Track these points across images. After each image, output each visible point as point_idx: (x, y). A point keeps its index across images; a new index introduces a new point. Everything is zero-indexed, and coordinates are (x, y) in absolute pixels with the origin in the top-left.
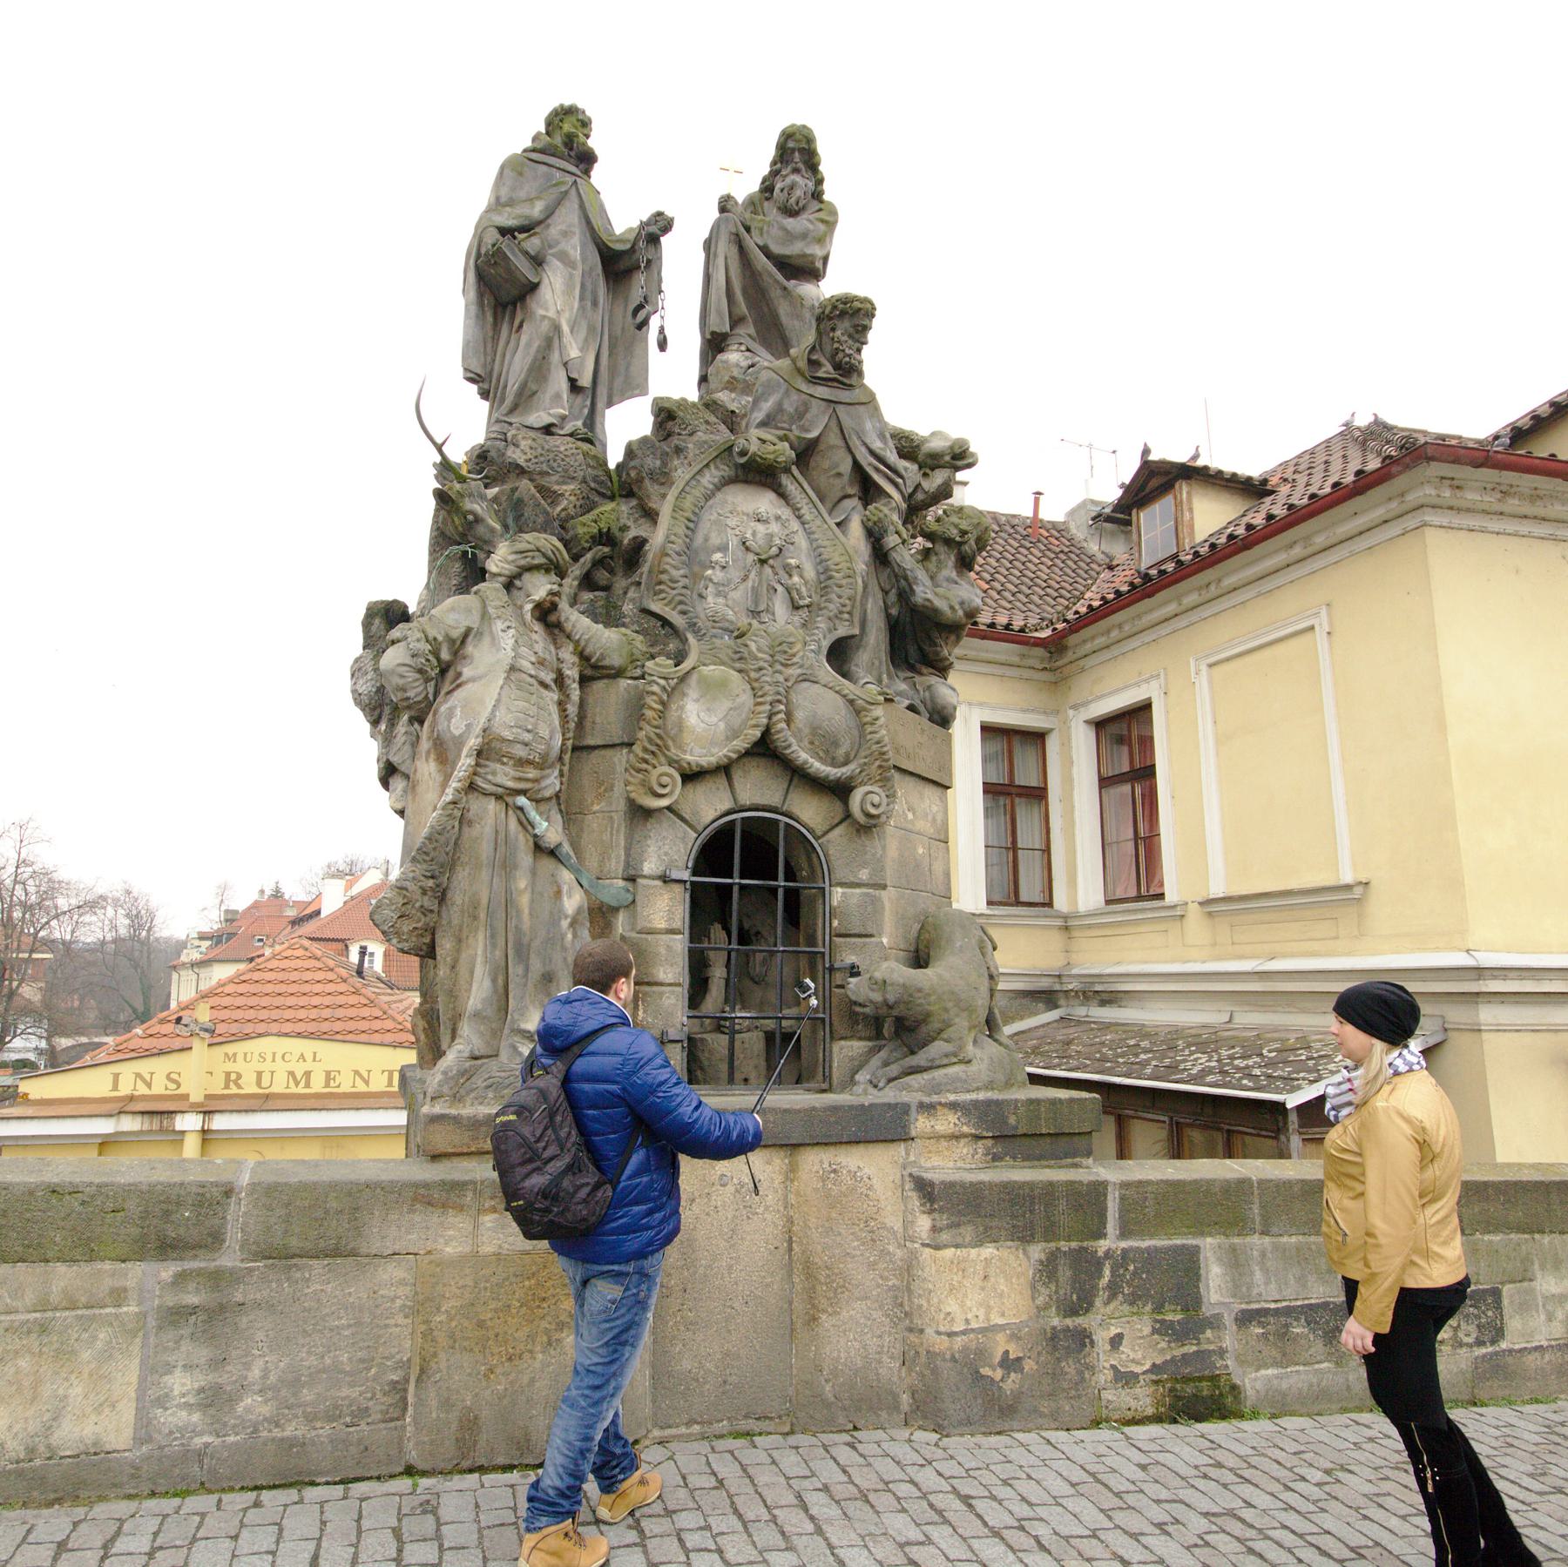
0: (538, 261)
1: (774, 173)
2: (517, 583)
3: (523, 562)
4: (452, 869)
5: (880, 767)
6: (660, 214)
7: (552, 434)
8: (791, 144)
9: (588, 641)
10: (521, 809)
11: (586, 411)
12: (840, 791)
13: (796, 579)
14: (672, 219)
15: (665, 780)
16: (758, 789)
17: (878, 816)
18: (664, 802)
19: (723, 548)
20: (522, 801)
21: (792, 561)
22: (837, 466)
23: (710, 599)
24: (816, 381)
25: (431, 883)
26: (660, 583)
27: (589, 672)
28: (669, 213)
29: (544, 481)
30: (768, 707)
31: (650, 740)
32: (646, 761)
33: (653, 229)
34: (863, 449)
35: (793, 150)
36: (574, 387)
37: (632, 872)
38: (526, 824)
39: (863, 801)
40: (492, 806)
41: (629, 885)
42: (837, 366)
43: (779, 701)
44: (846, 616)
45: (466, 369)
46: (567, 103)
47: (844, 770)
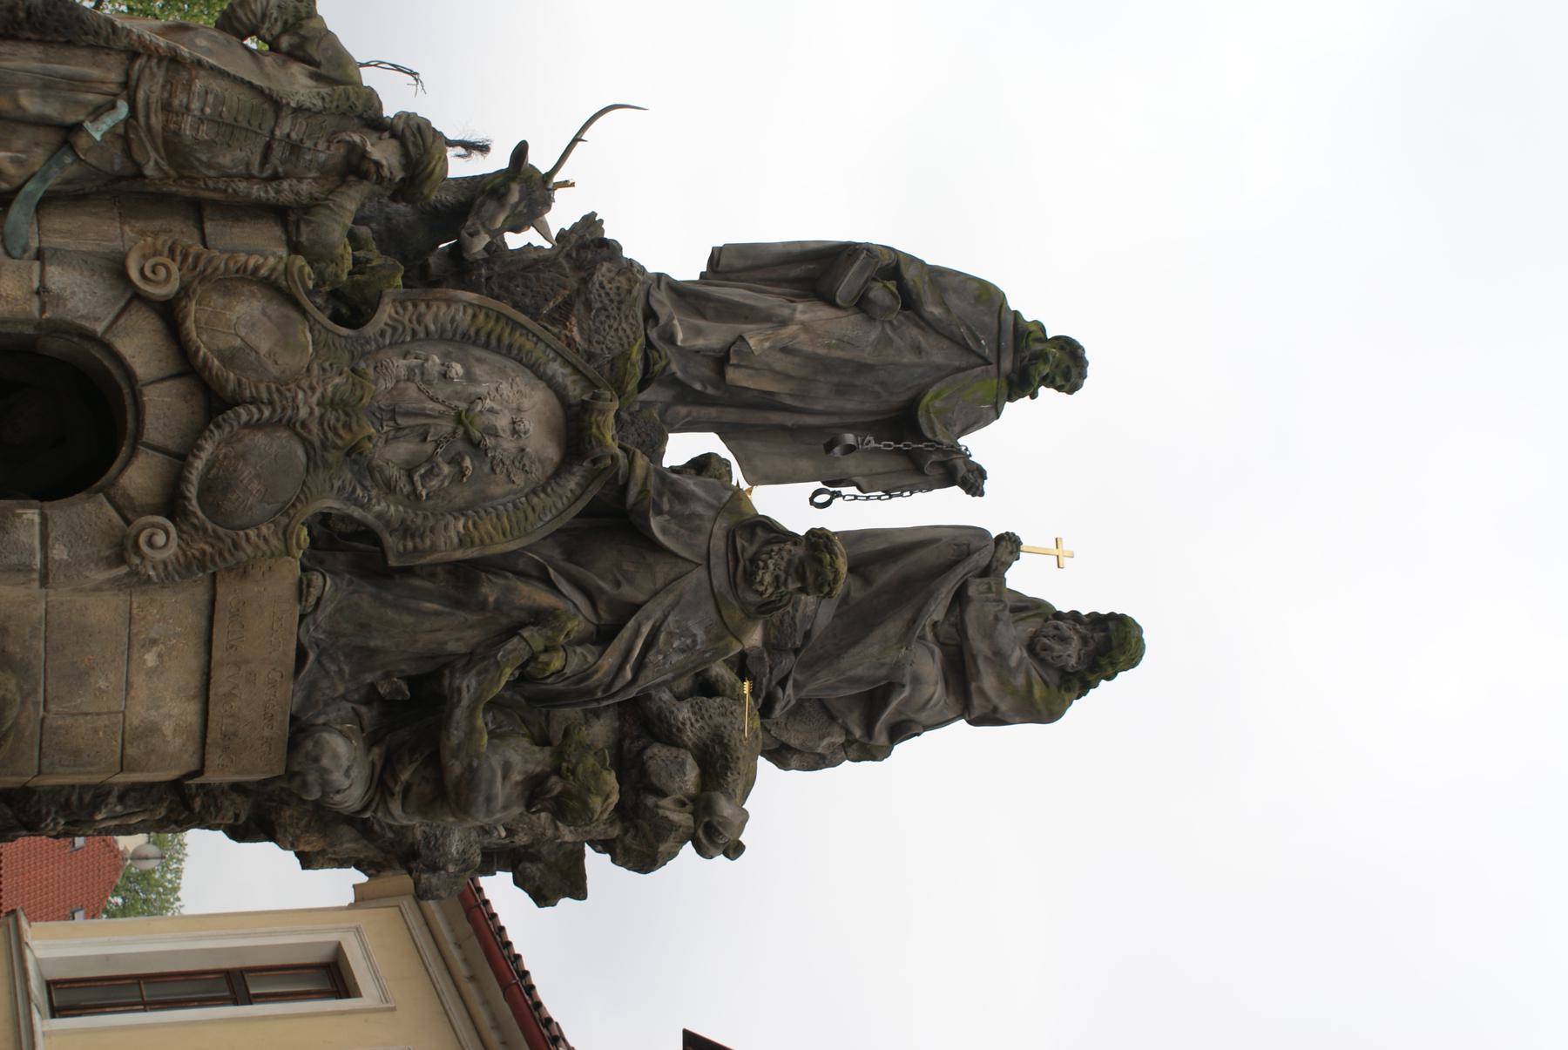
0: (862, 304)
1: (1075, 615)
2: (386, 134)
3: (408, 134)
4: (40, 42)
5: (204, 552)
6: (981, 474)
7: (646, 320)
8: (1111, 625)
9: (328, 207)
10: (113, 107)
11: (698, 386)
12: (172, 505)
13: (446, 469)
14: (982, 494)
15: (162, 272)
16: (163, 409)
17: (136, 546)
18: (134, 274)
19: (469, 377)
20: (123, 110)
21: (468, 462)
22: (631, 582)
23: (402, 362)
24: (731, 537)
25: (22, 14)
26: (415, 306)
27: (292, 217)
28: (987, 486)
29: (579, 306)
30: (265, 396)
31: (210, 260)
32: (185, 257)
33: (962, 471)
34: (658, 615)
35: (1105, 630)
36: (721, 360)
37: (48, 254)
38: (97, 113)
39: (154, 525)
40: (115, 76)
41: (32, 252)
42: (753, 560)
43: (274, 411)
44: (410, 545)
45: (720, 249)
46: (1088, 356)
47: (194, 502)
